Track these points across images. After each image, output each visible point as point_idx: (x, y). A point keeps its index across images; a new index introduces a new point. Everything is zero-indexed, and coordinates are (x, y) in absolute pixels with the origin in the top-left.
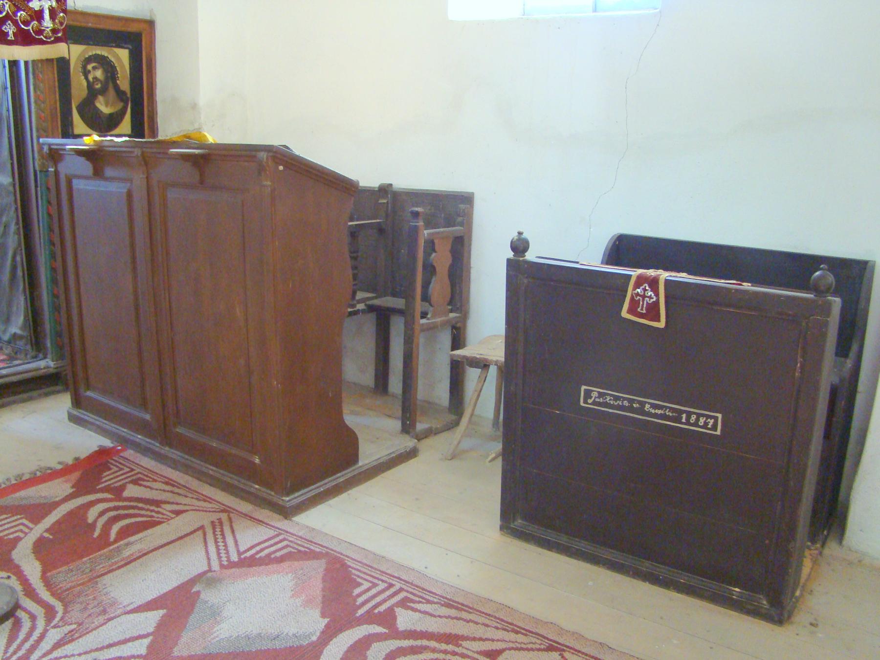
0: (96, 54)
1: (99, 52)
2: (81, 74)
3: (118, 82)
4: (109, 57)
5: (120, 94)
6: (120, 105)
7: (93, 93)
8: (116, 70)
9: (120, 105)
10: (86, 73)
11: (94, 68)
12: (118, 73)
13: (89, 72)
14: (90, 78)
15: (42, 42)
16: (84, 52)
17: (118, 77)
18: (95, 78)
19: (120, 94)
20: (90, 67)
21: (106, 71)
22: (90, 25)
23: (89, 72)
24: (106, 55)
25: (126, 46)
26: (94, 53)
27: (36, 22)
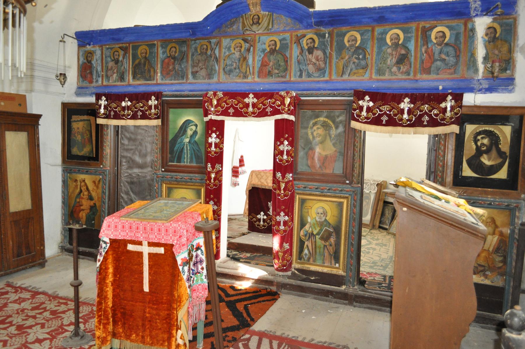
0: (485, 130)
1: (487, 129)
2: (472, 141)
3: (500, 146)
4: (495, 131)
5: (501, 154)
6: (499, 161)
7: (479, 152)
8: (500, 139)
9: (499, 161)
10: (476, 141)
11: (482, 138)
12: (500, 141)
13: (479, 140)
14: (479, 144)
15: (444, 125)
16: (475, 129)
17: (500, 143)
18: (483, 144)
19: (501, 154)
20: (479, 137)
21: (491, 140)
22: (482, 113)
23: (479, 140)
24: (492, 130)
25: (509, 124)
26: (483, 129)
27: (441, 114)
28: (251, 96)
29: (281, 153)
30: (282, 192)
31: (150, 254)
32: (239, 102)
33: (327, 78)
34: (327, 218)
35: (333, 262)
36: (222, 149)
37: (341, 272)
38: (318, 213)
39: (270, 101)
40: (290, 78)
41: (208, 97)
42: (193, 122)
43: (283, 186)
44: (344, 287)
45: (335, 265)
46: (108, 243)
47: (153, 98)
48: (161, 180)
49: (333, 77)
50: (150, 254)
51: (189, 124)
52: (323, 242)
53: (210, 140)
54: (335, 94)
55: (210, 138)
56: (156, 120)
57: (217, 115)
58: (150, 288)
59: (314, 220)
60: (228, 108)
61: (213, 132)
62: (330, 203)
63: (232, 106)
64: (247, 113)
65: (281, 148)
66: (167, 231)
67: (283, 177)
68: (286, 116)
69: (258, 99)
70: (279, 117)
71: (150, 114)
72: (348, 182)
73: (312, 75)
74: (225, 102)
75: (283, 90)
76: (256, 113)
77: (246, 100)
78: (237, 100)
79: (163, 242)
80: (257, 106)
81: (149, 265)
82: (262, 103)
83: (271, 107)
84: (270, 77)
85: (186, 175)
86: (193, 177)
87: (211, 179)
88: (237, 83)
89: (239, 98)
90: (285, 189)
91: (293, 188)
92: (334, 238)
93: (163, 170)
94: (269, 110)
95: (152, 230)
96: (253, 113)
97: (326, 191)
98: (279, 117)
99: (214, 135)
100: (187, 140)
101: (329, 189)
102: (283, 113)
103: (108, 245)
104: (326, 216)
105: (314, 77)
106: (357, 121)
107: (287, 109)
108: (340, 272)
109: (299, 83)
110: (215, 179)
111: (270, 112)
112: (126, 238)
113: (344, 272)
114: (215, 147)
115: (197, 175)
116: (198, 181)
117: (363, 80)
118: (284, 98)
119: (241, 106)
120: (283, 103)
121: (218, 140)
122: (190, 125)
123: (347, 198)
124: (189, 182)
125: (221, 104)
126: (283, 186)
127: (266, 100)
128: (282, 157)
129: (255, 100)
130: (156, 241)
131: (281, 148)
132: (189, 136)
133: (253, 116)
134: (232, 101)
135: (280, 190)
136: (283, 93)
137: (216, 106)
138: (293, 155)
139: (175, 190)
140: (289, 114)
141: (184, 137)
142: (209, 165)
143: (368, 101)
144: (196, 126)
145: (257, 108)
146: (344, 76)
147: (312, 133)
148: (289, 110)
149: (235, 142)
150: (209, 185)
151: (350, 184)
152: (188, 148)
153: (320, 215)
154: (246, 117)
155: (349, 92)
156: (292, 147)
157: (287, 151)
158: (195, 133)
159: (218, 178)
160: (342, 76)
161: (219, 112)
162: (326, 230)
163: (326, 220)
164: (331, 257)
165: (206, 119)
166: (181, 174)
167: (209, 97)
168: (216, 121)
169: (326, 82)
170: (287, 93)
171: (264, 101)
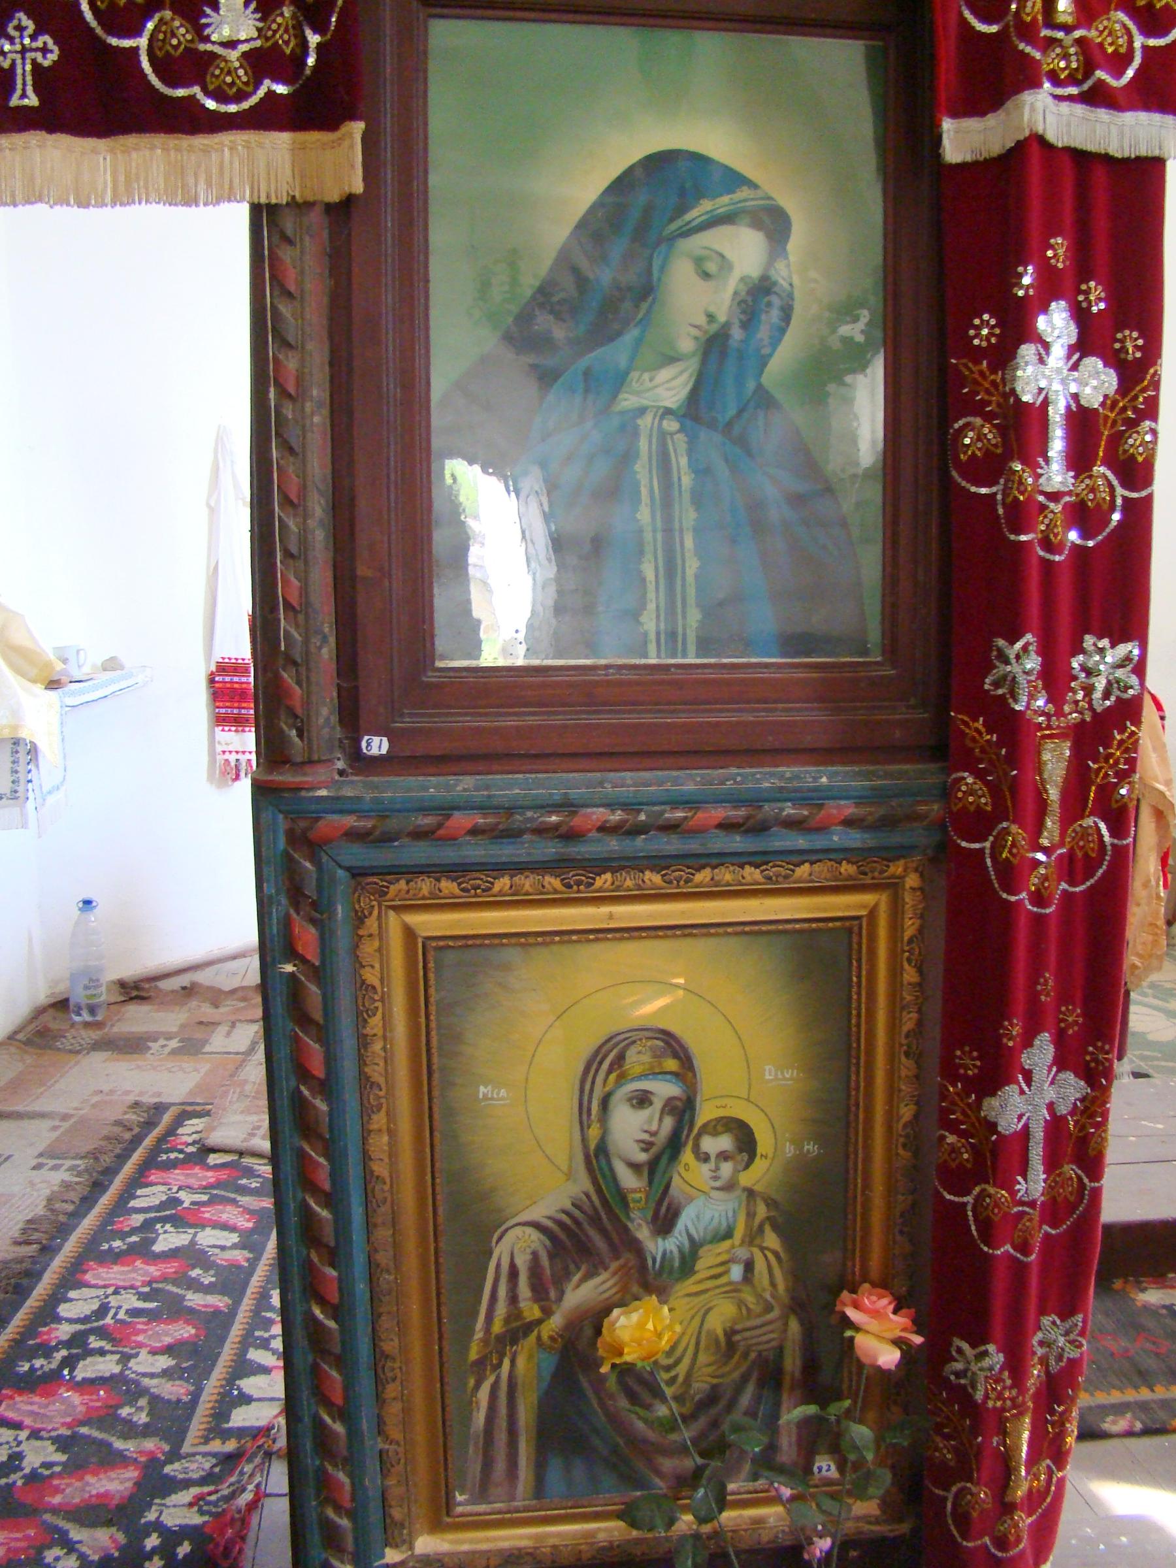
42: (735, 180)
48: (357, 873)
51: (682, 209)
56: (283, 139)
57: (1097, 97)
86: (779, 796)
93: (377, 746)
114: (1079, 461)
115: (823, 777)
116: (838, 837)
122: (696, 214)
124: (718, 859)
132: (686, 345)
149: (213, 511)
159: (1106, 791)
168: (1080, 158)
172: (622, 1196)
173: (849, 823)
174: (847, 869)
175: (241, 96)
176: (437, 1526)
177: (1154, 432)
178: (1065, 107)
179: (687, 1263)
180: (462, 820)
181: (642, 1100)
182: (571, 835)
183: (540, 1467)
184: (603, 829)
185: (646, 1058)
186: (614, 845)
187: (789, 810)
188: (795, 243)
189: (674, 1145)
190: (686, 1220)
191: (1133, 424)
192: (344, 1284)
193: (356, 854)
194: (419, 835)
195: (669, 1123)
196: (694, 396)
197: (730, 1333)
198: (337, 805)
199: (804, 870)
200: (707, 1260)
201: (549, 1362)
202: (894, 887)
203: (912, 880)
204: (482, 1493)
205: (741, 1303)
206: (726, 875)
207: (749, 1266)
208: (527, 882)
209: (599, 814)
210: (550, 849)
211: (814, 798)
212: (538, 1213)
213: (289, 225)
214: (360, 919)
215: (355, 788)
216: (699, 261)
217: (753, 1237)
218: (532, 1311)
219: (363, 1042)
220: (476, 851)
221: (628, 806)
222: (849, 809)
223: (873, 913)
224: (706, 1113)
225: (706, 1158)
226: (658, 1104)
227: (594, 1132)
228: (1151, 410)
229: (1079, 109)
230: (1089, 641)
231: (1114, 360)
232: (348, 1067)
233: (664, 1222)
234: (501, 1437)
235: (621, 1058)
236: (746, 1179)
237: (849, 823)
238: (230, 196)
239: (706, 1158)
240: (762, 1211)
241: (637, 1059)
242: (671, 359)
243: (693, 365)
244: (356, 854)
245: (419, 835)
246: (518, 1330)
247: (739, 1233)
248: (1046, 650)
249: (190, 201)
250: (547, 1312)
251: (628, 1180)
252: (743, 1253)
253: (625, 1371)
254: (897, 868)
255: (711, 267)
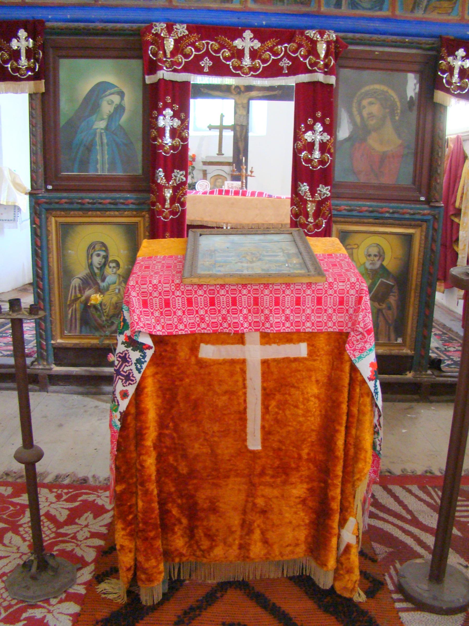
28: (248, 34)
29: (310, 147)
30: (311, 220)
31: (265, 363)
32: (222, 47)
33: (385, 13)
34: (385, 263)
35: (393, 336)
36: (185, 139)
37: (406, 351)
38: (370, 255)
39: (286, 48)
40: (319, 6)
41: (153, 34)
42: (115, 86)
43: (311, 208)
44: (409, 375)
45: (396, 340)
46: (149, 348)
47: (22, 33)
48: (47, 210)
49: (398, 13)
50: (265, 363)
51: (105, 91)
52: (376, 304)
53: (161, 122)
54: (405, 42)
55: (161, 118)
56: (32, 83)
57: (175, 71)
58: (264, 440)
59: (363, 266)
60: (199, 58)
61: (166, 106)
62: (392, 236)
63: (207, 53)
64: (239, 68)
65: (309, 136)
66: (319, 301)
67: (313, 191)
68: (320, 77)
69: (262, 41)
70: (303, 78)
71: (16, 70)
72: (422, 199)
73: (360, 6)
74: (193, 45)
75: (312, 28)
76: (258, 69)
77: (238, 43)
78: (219, 43)
79: (308, 327)
80: (260, 56)
81: (264, 389)
82: (271, 50)
83: (289, 58)
84: (279, 3)
85: (103, 195)
86: (119, 198)
87: (165, 200)
88: (209, 10)
89: (222, 38)
90: (317, 214)
91: (330, 213)
92: (394, 296)
93: (50, 187)
94: (285, 63)
95: (277, 303)
96: (253, 69)
97: (387, 215)
98: (303, 78)
99: (168, 112)
100: (102, 125)
101: (393, 213)
102: (315, 71)
103: (149, 353)
104: (383, 260)
105: (364, 9)
106: (447, 91)
107: (322, 63)
108: (404, 351)
109: (337, 17)
110: (173, 199)
111: (288, 68)
112: (197, 330)
113: (411, 350)
116: (131, 206)
117: (448, 21)
118: (314, 43)
119: (228, 54)
120: (313, 51)
121: (176, 123)
122: (107, 93)
123: (421, 226)
124: (110, 210)
125: (183, 50)
126: (311, 208)
127: (278, 44)
128: (311, 154)
129: (257, 44)
130: (287, 328)
131: (309, 136)
132: (105, 117)
133: (252, 76)
134: (208, 44)
135: (307, 216)
136: (311, 33)
137: (173, 54)
138: (332, 151)
139: (79, 229)
140: (326, 73)
141: (94, 117)
142: (161, 173)
143: (462, 58)
144: (122, 94)
145: (260, 58)
146: (416, 12)
147: (360, 114)
148: (326, 65)
150: (161, 213)
151: (428, 202)
152: (105, 141)
153: (372, 258)
154: (238, 75)
155: (430, 40)
156: (331, 137)
157: (320, 144)
158: (120, 109)
159: (180, 199)
160: (412, 11)
161: (180, 64)
162: (382, 283)
163: (382, 266)
164: (389, 328)
165: (149, 79)
166: (93, 195)
167: (157, 35)
169: (385, 20)
170: (322, 35)
171: (274, 46)
172: (95, 274)
173: (132, 203)
174: (135, 213)
175: (25, 75)
176: (62, 338)
177: (188, 133)
178: (169, 73)
179: (108, 289)
180: (64, 201)
181: (98, 255)
182: (83, 204)
183: (81, 327)
184: (89, 203)
185: (99, 247)
186: (90, 206)
187: (122, 201)
188: (126, 98)
189: (105, 264)
190: (107, 279)
191: (183, 130)
192: (43, 285)
193: (47, 206)
194: (57, 203)
195: (104, 260)
196: (107, 125)
197: (116, 303)
198: (43, 197)
199: (126, 213)
200: (112, 287)
201: (82, 306)
202: (143, 216)
203: (147, 216)
204: (70, 332)
205: (118, 297)
206: (112, 213)
207: (119, 290)
208: (76, 213)
209: (88, 200)
210: (79, 206)
211: (127, 199)
212: (80, 276)
213: (34, 97)
214: (47, 218)
215: (47, 195)
216: (108, 102)
217: (120, 284)
218: (79, 295)
219: (48, 241)
220: (66, 206)
221: (93, 199)
222: (132, 201)
223: (140, 221)
224: (110, 259)
225: (110, 267)
226: (101, 256)
227: (90, 261)
228: (187, 128)
229: (172, 73)
230: (175, 171)
231: (179, 118)
232: (45, 243)
233: (103, 280)
234: (74, 321)
235: (94, 247)
236: (119, 272)
237: (132, 203)
238: (23, 92)
239: (110, 267)
240: (121, 279)
241: (97, 247)
242: (102, 119)
243: (107, 120)
244: (47, 206)
245: (57, 203)
246: (76, 299)
247: (117, 282)
248: (164, 171)
249: (17, 93)
250: (82, 296)
251: (96, 271)
252: (118, 287)
253: (95, 306)
254: (144, 213)
255: (110, 102)
